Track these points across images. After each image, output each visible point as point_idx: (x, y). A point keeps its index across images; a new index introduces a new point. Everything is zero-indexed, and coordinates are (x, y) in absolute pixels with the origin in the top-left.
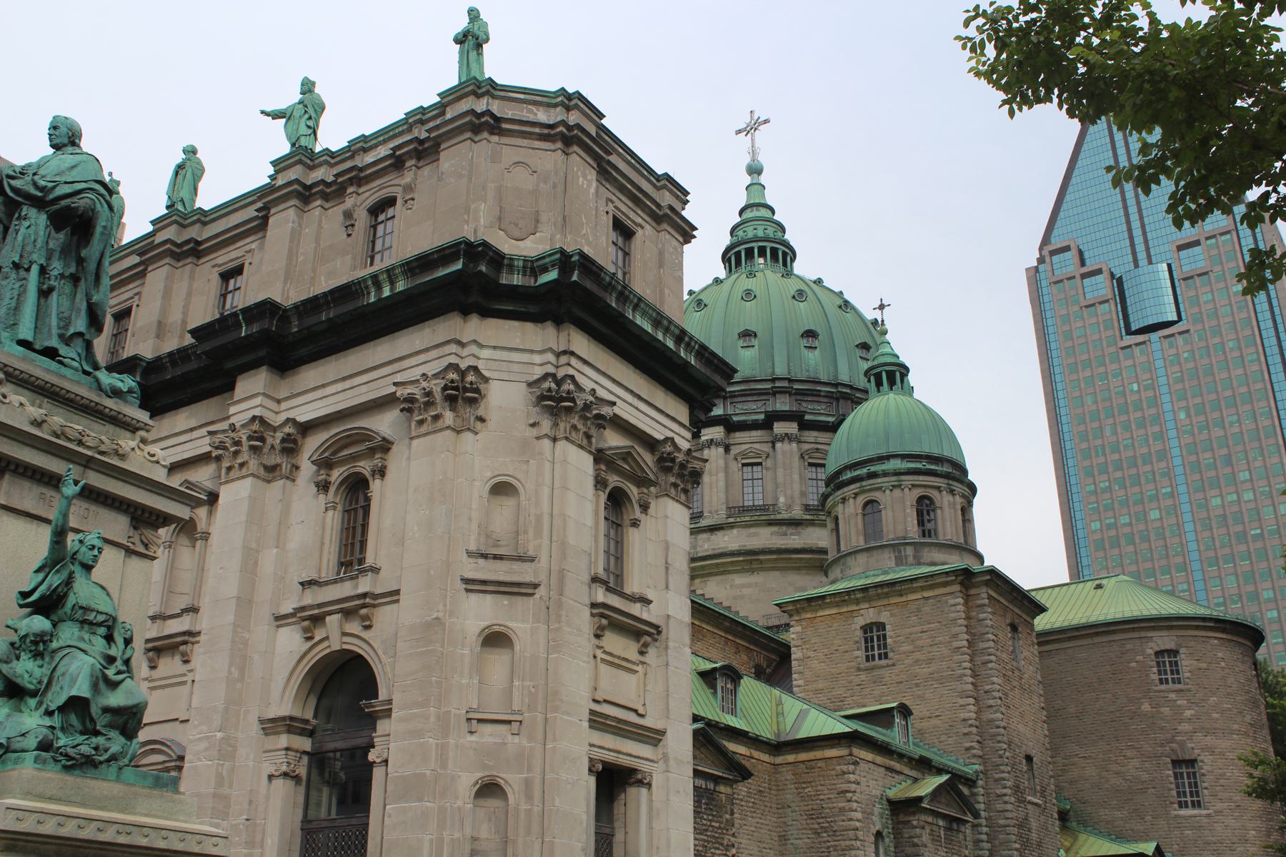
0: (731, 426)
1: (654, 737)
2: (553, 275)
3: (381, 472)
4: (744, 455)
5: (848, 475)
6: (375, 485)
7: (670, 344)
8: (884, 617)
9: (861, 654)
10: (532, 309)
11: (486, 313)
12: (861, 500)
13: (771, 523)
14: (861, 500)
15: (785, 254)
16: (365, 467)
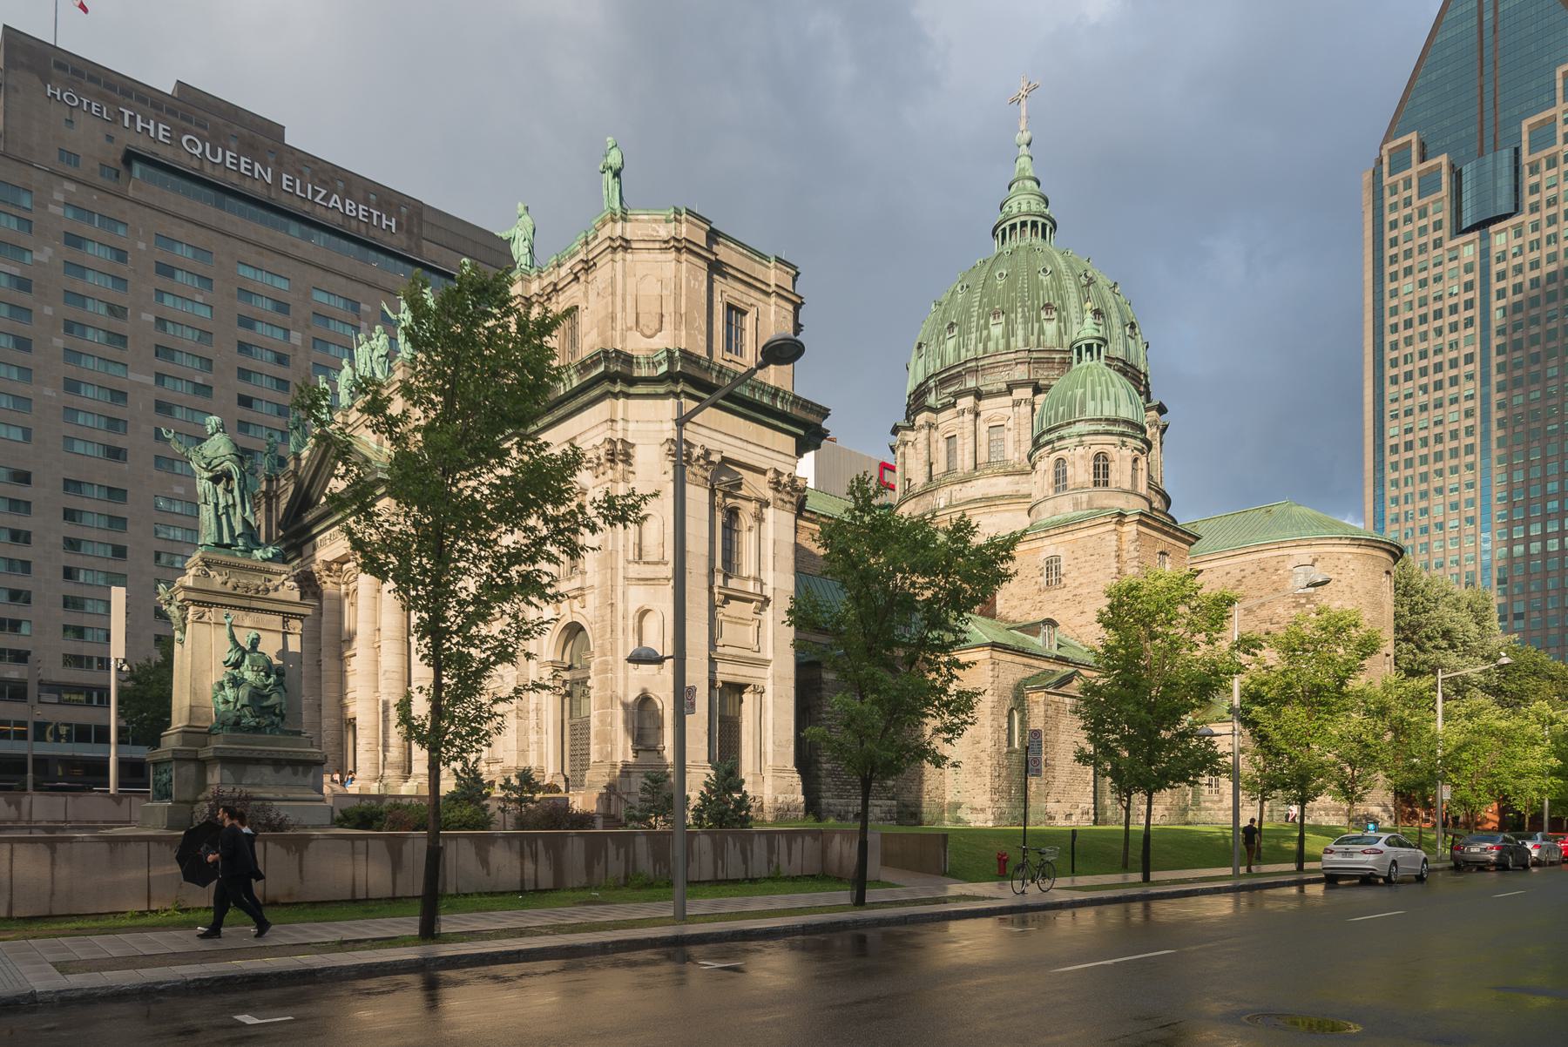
1: (764, 663)
5: (1046, 438)
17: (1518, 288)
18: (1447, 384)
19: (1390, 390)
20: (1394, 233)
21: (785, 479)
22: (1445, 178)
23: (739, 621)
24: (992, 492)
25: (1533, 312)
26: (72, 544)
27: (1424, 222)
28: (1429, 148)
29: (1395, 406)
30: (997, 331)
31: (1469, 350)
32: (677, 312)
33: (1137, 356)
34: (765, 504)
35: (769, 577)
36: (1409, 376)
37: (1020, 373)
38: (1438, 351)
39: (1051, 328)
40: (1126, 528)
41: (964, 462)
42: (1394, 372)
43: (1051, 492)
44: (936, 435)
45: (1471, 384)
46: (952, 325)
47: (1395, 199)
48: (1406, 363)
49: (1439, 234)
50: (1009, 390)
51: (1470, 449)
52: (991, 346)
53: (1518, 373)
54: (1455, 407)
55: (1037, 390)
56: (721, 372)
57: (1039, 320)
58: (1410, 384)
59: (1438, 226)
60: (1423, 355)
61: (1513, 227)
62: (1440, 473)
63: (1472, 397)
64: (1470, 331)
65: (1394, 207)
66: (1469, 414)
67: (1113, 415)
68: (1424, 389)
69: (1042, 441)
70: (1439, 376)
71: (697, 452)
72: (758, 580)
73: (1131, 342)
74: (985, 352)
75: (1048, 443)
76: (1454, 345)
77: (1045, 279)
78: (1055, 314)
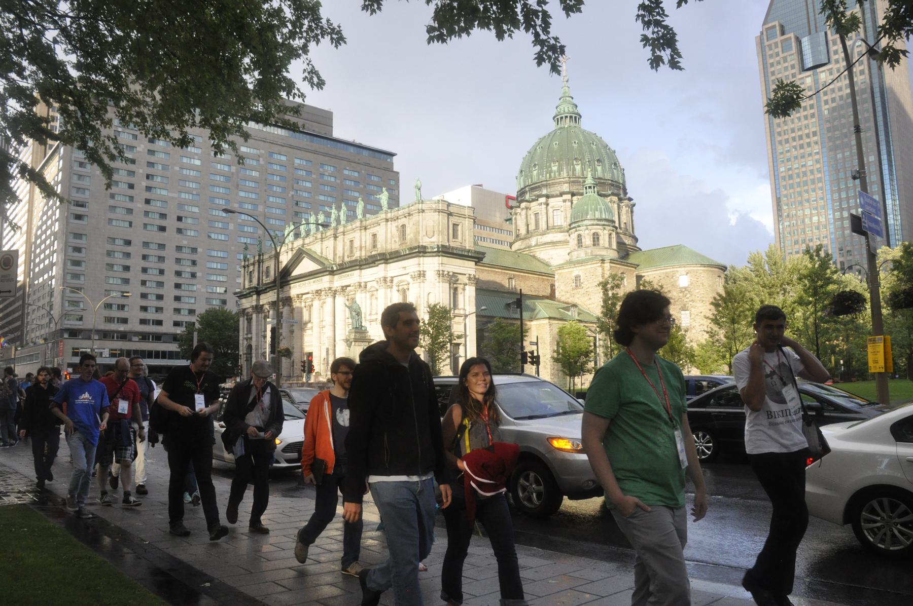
0: (548, 197)
2: (436, 250)
3: (408, 289)
4: (553, 207)
5: (572, 226)
6: (407, 292)
7: (466, 254)
8: (580, 273)
9: (574, 285)
10: (434, 254)
11: (424, 256)
12: (577, 233)
13: (561, 232)
14: (577, 233)
15: (575, 117)
16: (405, 287)
17: (833, 100)
18: (805, 146)
19: (780, 149)
20: (773, 69)
21: (472, 276)
22: (794, 44)
23: (459, 323)
24: (555, 240)
25: (842, 112)
26: (145, 270)
27: (786, 65)
28: (786, 28)
29: (782, 156)
30: (555, 168)
31: (814, 129)
32: (439, 231)
33: (618, 177)
34: (466, 284)
35: (467, 308)
36: (787, 141)
37: (565, 188)
38: (800, 129)
39: (578, 168)
40: (605, 265)
41: (543, 225)
42: (779, 138)
43: (576, 248)
44: (529, 212)
45: (816, 147)
46: (535, 165)
47: (771, 52)
48: (785, 134)
49: (794, 71)
50: (561, 195)
51: (820, 180)
52: (553, 174)
53: (838, 142)
54: (810, 158)
55: (573, 195)
56: (453, 248)
57: (573, 164)
58: (787, 145)
59: (793, 67)
60: (793, 131)
61: (828, 70)
62: (807, 191)
63: (817, 153)
64: (814, 120)
65: (771, 56)
66: (817, 161)
67: (599, 217)
68: (795, 147)
69: (572, 226)
70: (801, 142)
71: (446, 273)
72: (464, 309)
73: (615, 171)
74: (550, 177)
75: (574, 228)
76: (807, 126)
77: (575, 146)
78: (580, 162)
